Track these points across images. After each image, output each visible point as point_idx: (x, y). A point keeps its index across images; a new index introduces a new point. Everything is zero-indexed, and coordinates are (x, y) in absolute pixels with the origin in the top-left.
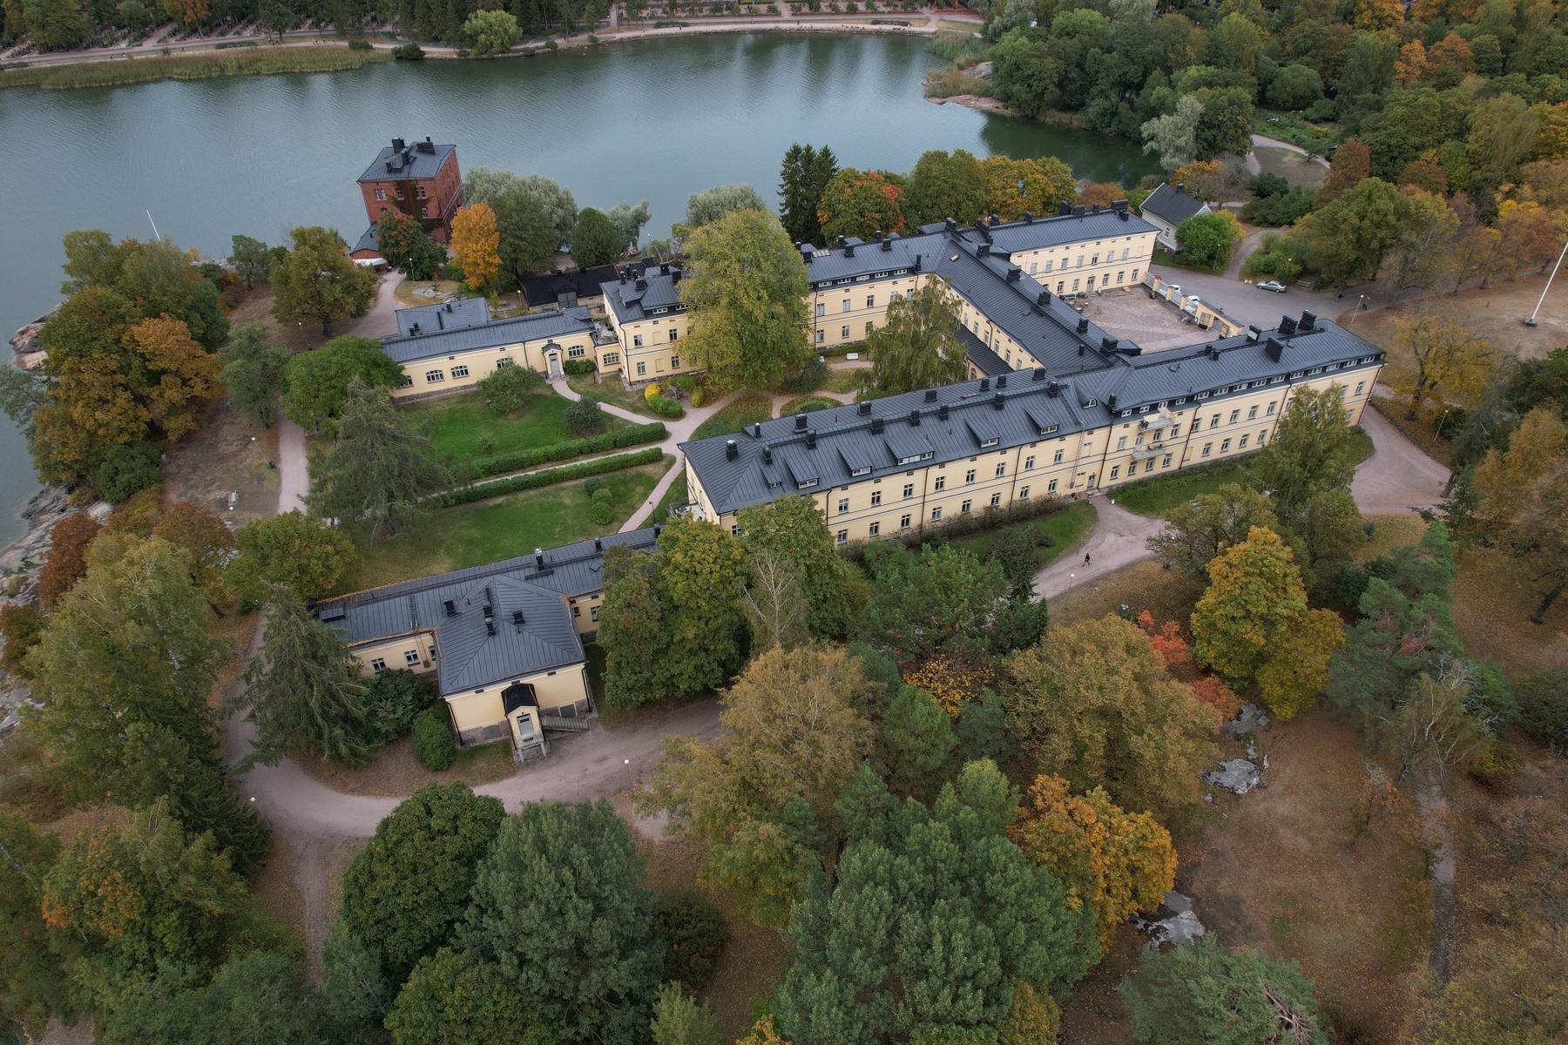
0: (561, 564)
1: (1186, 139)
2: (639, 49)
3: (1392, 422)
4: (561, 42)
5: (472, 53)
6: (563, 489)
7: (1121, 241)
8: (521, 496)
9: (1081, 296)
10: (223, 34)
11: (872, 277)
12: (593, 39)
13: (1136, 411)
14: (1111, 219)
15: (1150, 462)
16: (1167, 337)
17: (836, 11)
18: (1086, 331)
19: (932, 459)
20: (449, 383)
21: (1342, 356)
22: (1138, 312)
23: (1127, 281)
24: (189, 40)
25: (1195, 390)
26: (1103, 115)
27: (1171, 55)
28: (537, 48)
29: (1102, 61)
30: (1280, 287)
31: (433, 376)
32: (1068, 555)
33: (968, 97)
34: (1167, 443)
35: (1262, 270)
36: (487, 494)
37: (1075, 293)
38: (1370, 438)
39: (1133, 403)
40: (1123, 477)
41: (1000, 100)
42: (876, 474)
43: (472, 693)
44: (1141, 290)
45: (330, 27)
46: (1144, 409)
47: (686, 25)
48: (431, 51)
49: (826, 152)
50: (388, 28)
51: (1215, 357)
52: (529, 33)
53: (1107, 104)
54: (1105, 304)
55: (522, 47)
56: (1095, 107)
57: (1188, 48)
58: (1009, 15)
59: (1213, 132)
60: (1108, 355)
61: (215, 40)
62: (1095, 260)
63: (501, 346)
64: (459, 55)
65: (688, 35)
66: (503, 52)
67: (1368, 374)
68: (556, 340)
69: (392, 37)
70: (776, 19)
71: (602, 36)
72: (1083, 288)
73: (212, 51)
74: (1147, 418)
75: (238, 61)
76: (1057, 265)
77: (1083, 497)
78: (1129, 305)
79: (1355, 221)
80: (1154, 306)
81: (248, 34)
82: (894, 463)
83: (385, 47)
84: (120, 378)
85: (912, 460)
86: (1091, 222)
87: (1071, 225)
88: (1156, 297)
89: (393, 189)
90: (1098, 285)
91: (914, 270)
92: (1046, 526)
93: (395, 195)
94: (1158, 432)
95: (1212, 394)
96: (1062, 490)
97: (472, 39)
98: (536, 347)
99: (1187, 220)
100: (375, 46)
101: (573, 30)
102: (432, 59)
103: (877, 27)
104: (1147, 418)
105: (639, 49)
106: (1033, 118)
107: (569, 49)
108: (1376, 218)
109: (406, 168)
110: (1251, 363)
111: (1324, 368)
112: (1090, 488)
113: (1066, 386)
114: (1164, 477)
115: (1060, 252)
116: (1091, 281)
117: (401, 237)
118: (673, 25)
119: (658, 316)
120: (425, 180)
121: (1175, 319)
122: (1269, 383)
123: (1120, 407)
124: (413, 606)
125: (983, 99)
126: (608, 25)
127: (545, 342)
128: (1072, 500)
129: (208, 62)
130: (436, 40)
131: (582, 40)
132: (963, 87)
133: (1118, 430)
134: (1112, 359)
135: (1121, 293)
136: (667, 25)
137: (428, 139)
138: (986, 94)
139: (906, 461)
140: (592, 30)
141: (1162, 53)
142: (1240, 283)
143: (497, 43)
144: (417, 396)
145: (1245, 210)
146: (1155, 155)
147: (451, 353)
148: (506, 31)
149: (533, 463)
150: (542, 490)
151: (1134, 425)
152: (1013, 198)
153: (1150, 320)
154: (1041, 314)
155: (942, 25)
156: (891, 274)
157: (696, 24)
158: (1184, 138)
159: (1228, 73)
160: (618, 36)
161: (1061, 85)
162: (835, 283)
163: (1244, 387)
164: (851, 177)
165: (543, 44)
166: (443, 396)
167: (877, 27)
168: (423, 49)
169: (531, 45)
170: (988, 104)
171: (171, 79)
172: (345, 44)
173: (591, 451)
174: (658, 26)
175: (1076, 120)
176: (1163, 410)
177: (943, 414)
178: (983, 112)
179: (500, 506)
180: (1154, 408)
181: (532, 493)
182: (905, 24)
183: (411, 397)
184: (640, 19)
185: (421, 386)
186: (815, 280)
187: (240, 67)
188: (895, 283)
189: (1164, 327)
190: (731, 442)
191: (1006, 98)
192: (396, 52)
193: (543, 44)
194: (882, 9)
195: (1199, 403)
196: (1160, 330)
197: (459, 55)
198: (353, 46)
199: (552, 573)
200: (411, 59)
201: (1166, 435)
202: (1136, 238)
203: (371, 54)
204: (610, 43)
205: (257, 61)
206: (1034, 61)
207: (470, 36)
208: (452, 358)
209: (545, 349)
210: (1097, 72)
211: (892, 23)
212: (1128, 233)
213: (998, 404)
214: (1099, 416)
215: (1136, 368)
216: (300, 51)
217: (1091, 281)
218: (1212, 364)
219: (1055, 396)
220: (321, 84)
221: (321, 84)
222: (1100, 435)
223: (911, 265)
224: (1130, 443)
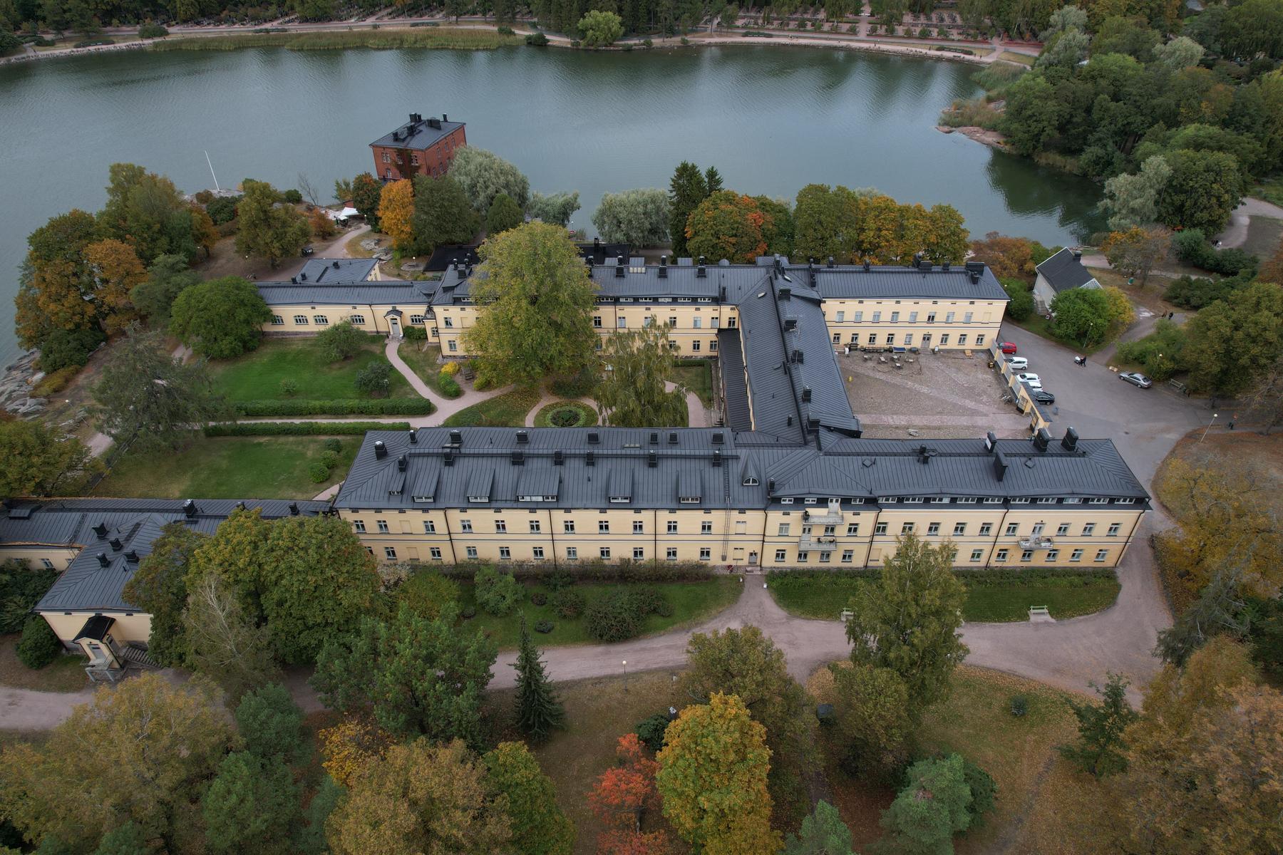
0: (207, 517)
1: (1145, 201)
2: (730, 54)
3: (1162, 573)
4: (657, 41)
6: (316, 442)
7: (962, 306)
8: (282, 439)
9: (914, 351)
11: (675, 301)
12: (684, 42)
13: (799, 502)
14: (961, 281)
15: (826, 555)
16: (974, 413)
17: (909, 35)
18: (809, 401)
19: (557, 501)
20: (312, 327)
21: (1087, 490)
22: (961, 378)
23: (970, 344)
25: (876, 493)
26: (1096, 163)
27: (1182, 110)
28: (635, 45)
29: (1107, 110)
30: (1142, 382)
31: (300, 320)
32: (676, 631)
33: (976, 129)
34: (838, 540)
35: (1134, 360)
36: (254, 432)
37: (909, 347)
38: (1118, 587)
39: (797, 491)
40: (791, 561)
41: (1005, 135)
42: (494, 505)
43: (63, 614)
44: (984, 356)
46: (810, 500)
47: (770, 36)
48: (555, 40)
49: (712, 174)
51: (925, 461)
52: (632, 31)
53: (1101, 152)
54: (935, 364)
56: (1092, 152)
57: (1203, 105)
58: (1058, 53)
59: (1183, 197)
60: (810, 432)
61: (415, 20)
62: (931, 318)
63: (354, 305)
64: (573, 44)
65: (768, 45)
66: (606, 46)
67: (1127, 518)
68: (399, 308)
69: (534, 26)
71: (693, 39)
72: (917, 343)
74: (811, 511)
76: (887, 316)
77: (740, 572)
78: (959, 369)
79: (1226, 331)
80: (989, 377)
82: (516, 502)
83: (522, 33)
84: (74, 280)
85: (534, 499)
86: (935, 280)
87: (916, 280)
88: (995, 366)
90: (935, 343)
91: (719, 300)
92: (675, 593)
94: (830, 529)
95: (901, 502)
96: (714, 560)
97: (583, 33)
98: (382, 310)
99: (1070, 292)
100: (517, 32)
101: (671, 32)
102: (554, 46)
103: (939, 53)
104: (811, 511)
106: (1029, 156)
108: (1252, 331)
110: (972, 475)
111: (1060, 501)
112: (752, 564)
113: (737, 458)
114: (839, 572)
115: (888, 306)
116: (927, 338)
117: (366, 197)
118: (759, 35)
119: (469, 304)
120: (418, 150)
121: (996, 393)
122: (980, 502)
123: (779, 494)
124: (81, 523)
125: (989, 133)
127: (389, 308)
128: (727, 572)
130: (559, 32)
131: (675, 41)
132: (976, 119)
133: (776, 517)
134: (810, 437)
135: (961, 355)
136: (753, 35)
138: (993, 128)
139: (527, 499)
141: (1173, 107)
142: (1105, 369)
144: (288, 333)
145: (1177, 286)
146: (1107, 213)
147: (313, 304)
148: (610, 29)
149: (311, 413)
150: (300, 438)
151: (796, 515)
152: (888, 241)
153: (971, 392)
154: (787, 371)
155: (1004, 56)
156: (694, 300)
157: (778, 36)
158: (1139, 201)
159: (1229, 135)
161: (1062, 128)
162: (636, 301)
163: (946, 501)
164: (730, 199)
166: (305, 337)
167: (939, 53)
168: (548, 37)
169: (631, 42)
170: (991, 138)
172: (496, 29)
173: (362, 413)
174: (745, 35)
175: (1071, 165)
176: (835, 506)
177: (590, 460)
178: (988, 145)
179: (260, 444)
180: (822, 502)
181: (291, 439)
182: (970, 53)
183: (283, 333)
185: (290, 326)
186: (618, 295)
188: (698, 309)
189: (981, 402)
190: (378, 443)
191: (1007, 134)
192: (529, 38)
194: (956, 37)
195: (879, 508)
196: (970, 404)
198: (501, 31)
199: (196, 522)
200: (538, 44)
201: (841, 532)
202: (981, 305)
206: (1036, 102)
208: (313, 308)
209: (389, 313)
210: (1102, 119)
211: (956, 51)
212: (972, 297)
213: (653, 461)
214: (756, 495)
215: (826, 454)
217: (927, 338)
218: (919, 466)
219: (719, 465)
220: (481, 57)
221: (481, 57)
222: (753, 519)
223: (716, 294)
224: (796, 529)
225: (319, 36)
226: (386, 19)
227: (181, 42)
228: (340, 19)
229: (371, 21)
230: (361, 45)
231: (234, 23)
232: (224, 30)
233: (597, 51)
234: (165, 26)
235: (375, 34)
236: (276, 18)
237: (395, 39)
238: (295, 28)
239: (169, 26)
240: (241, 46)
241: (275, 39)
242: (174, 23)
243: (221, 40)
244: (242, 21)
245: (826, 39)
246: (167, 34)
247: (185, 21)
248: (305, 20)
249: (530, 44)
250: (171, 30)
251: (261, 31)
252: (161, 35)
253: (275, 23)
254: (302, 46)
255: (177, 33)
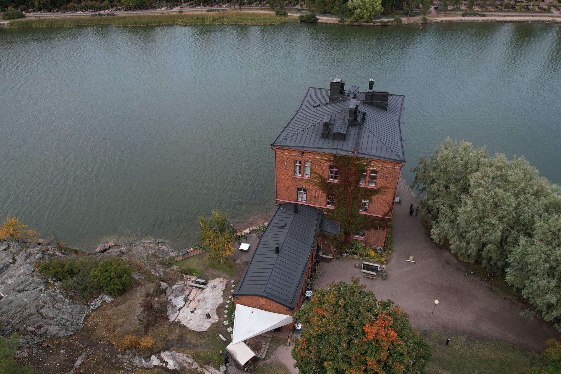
4: (404, 20)
5: (348, 21)
10: (212, 6)
12: (425, 20)
24: (195, 8)
28: (389, 22)
45: (267, 5)
47: (484, 16)
48: (322, 19)
50: (298, 7)
55: (380, 20)
61: (208, 8)
66: (368, 22)
69: (299, 10)
70: (550, 15)
71: (430, 19)
73: (204, 13)
75: (214, 18)
81: (224, 6)
83: (294, 15)
89: (325, 166)
93: (326, 174)
97: (350, 12)
102: (322, 23)
105: (449, 28)
107: (409, 24)
109: (353, 132)
118: (475, 15)
126: (430, 12)
129: (198, 18)
130: (325, 13)
131: (417, 19)
136: (471, 15)
137: (371, 84)
140: (425, 14)
143: (366, 16)
148: (374, 8)
157: (491, 16)
160: (440, 19)
165: (393, 19)
169: (386, 20)
171: (177, 24)
174: (464, 15)
184: (448, 11)
187: (214, 21)
193: (393, 19)
197: (340, 21)
198: (278, 13)
203: (287, 18)
204: (434, 23)
205: (224, 18)
207: (350, 10)
216: (248, 14)
225: (139, 17)
226: (187, 8)
227: (33, 21)
228: (155, 8)
229: (176, 9)
230: (171, 22)
231: (77, 11)
232: (68, 15)
233: (360, 26)
234: (24, 13)
235: (181, 16)
236: (108, 8)
237: (198, 19)
238: (122, 13)
239: (27, 12)
240: (80, 25)
241: (106, 20)
242: (31, 10)
243: (64, 21)
244: (83, 9)
245: (532, 16)
246: (24, 17)
247: (40, 9)
248: (129, 8)
249: (302, 21)
250: (28, 14)
251: (96, 15)
252: (19, 18)
253: (107, 11)
254: (127, 24)
255: (31, 16)
